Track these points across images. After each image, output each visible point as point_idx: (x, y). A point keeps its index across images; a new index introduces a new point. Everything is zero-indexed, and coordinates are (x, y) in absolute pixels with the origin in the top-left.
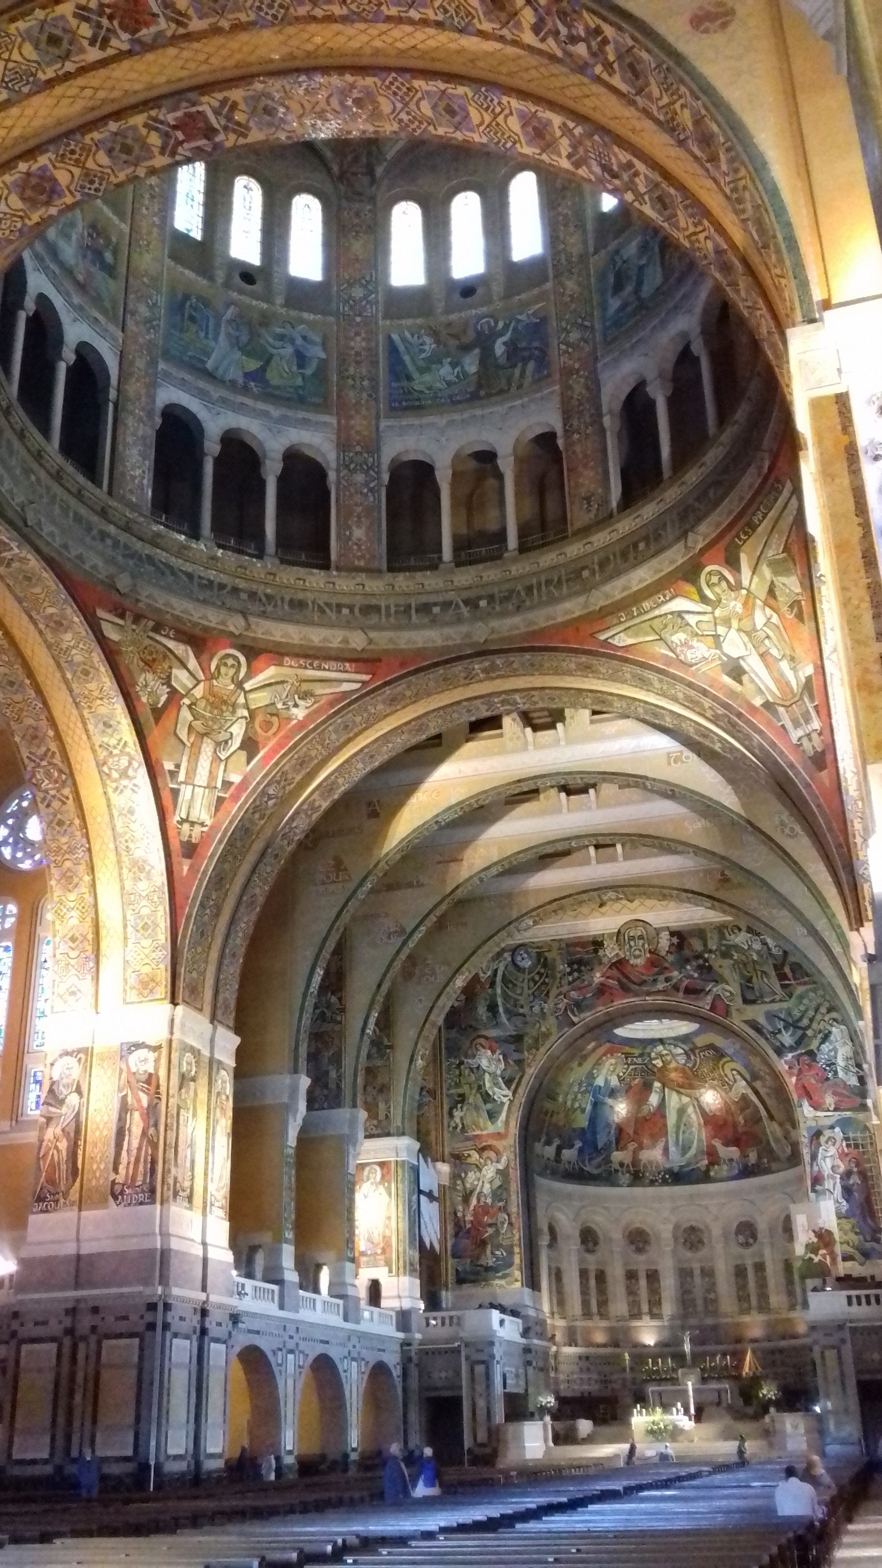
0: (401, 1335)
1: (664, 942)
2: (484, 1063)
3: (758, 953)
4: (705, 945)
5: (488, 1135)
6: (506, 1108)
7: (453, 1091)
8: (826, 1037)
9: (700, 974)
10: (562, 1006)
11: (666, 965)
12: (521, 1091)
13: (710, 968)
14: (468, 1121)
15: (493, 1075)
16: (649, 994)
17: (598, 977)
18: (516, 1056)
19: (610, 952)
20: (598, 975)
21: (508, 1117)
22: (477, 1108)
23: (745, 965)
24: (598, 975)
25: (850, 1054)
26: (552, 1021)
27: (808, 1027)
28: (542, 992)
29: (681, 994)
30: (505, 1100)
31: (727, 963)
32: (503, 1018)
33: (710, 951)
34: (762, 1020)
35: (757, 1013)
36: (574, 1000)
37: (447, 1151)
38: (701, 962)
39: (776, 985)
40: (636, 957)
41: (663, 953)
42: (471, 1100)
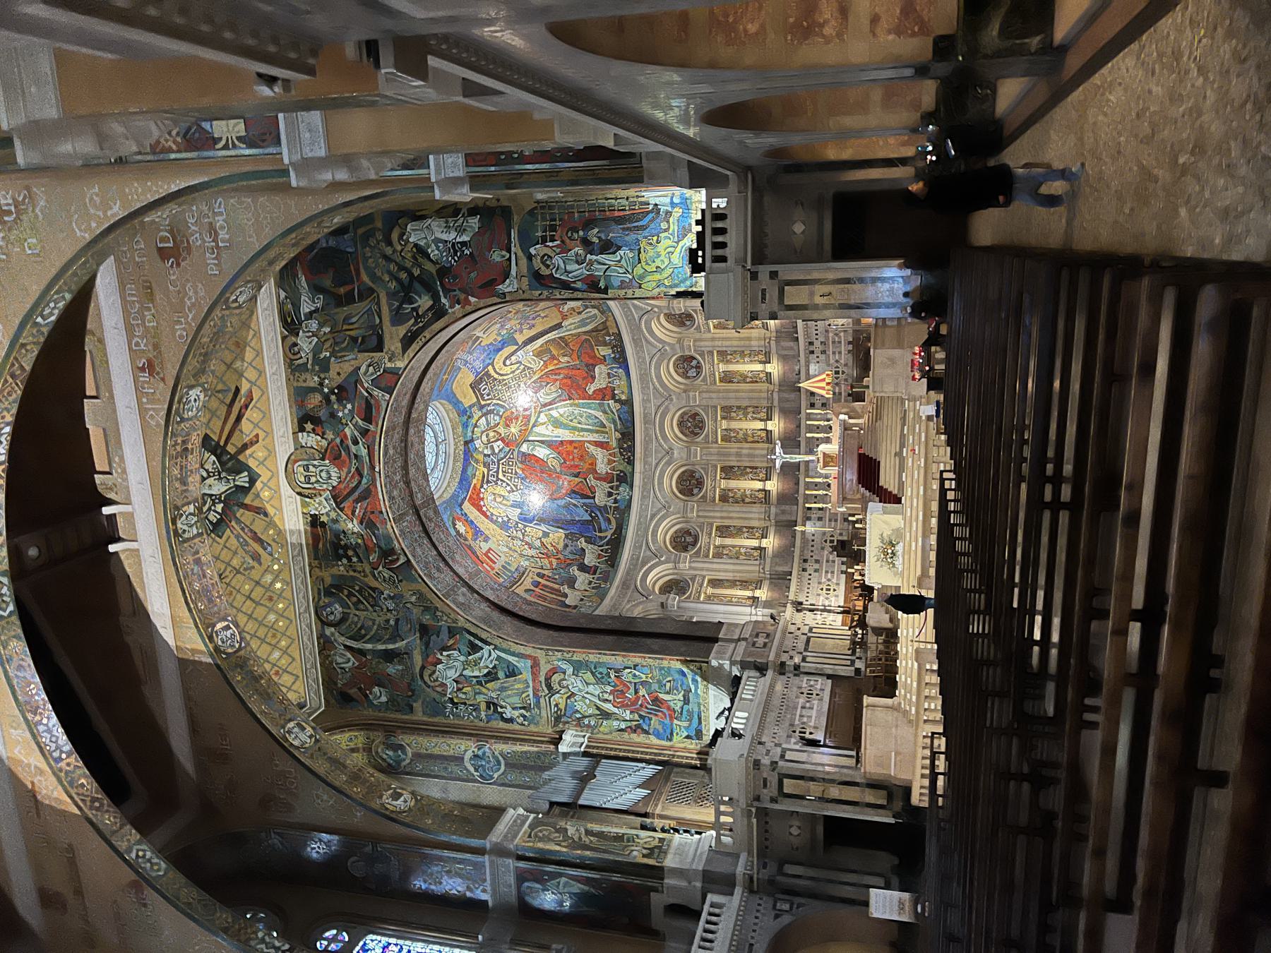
0: (738, 891)
1: (310, 440)
2: (452, 674)
3: (321, 325)
4: (313, 390)
5: (534, 680)
6: (503, 655)
7: (483, 714)
8: (421, 251)
9: (349, 401)
10: (386, 574)
11: (338, 440)
12: (484, 635)
13: (339, 387)
14: (515, 700)
15: (466, 664)
16: (373, 468)
17: (353, 526)
18: (444, 634)
19: (323, 507)
20: (350, 526)
21: (513, 654)
22: (503, 689)
23: (336, 343)
24: (350, 526)
25: (442, 222)
26: (404, 588)
27: (410, 274)
28: (371, 596)
29: (372, 428)
30: (494, 655)
31: (334, 366)
32: (400, 645)
33: (321, 384)
34: (402, 330)
35: (394, 335)
36: (380, 558)
37: (550, 731)
38: (333, 398)
39: (361, 307)
40: (329, 478)
41: (324, 443)
42: (494, 695)
